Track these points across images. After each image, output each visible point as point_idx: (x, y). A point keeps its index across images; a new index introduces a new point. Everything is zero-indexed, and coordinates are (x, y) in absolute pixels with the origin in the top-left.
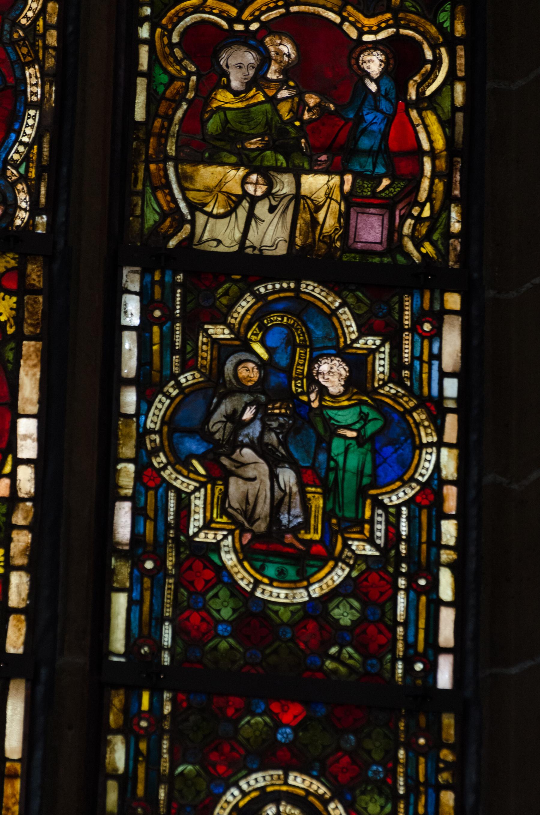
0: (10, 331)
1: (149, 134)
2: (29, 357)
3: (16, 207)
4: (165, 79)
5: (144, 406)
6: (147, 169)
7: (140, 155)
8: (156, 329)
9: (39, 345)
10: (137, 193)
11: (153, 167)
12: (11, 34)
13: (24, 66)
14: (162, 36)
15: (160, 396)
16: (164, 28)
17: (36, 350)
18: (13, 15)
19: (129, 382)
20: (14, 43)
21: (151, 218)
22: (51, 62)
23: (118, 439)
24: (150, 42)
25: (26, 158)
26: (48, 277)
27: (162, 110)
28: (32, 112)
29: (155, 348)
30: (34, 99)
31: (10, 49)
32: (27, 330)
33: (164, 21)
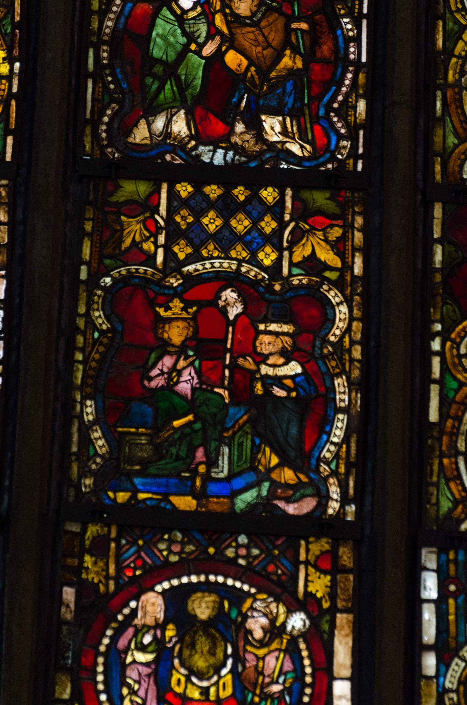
0: (326, 605)
1: (442, 433)
2: (342, 628)
3: (329, 498)
4: (454, 385)
5: (443, 668)
6: (441, 463)
7: (434, 451)
8: (451, 602)
9: (351, 617)
10: (433, 484)
11: (446, 461)
12: (321, 349)
13: (333, 377)
14: (452, 348)
15: (456, 660)
16: (453, 341)
17: (348, 621)
18: (323, 333)
19: (429, 648)
20: (324, 357)
21: (445, 505)
22: (356, 373)
23: (420, 697)
24: (442, 354)
25: (337, 456)
26: (357, 558)
27: (453, 412)
28: (341, 416)
29: (451, 618)
30: (342, 405)
31: (320, 363)
32: (340, 604)
33: (453, 336)
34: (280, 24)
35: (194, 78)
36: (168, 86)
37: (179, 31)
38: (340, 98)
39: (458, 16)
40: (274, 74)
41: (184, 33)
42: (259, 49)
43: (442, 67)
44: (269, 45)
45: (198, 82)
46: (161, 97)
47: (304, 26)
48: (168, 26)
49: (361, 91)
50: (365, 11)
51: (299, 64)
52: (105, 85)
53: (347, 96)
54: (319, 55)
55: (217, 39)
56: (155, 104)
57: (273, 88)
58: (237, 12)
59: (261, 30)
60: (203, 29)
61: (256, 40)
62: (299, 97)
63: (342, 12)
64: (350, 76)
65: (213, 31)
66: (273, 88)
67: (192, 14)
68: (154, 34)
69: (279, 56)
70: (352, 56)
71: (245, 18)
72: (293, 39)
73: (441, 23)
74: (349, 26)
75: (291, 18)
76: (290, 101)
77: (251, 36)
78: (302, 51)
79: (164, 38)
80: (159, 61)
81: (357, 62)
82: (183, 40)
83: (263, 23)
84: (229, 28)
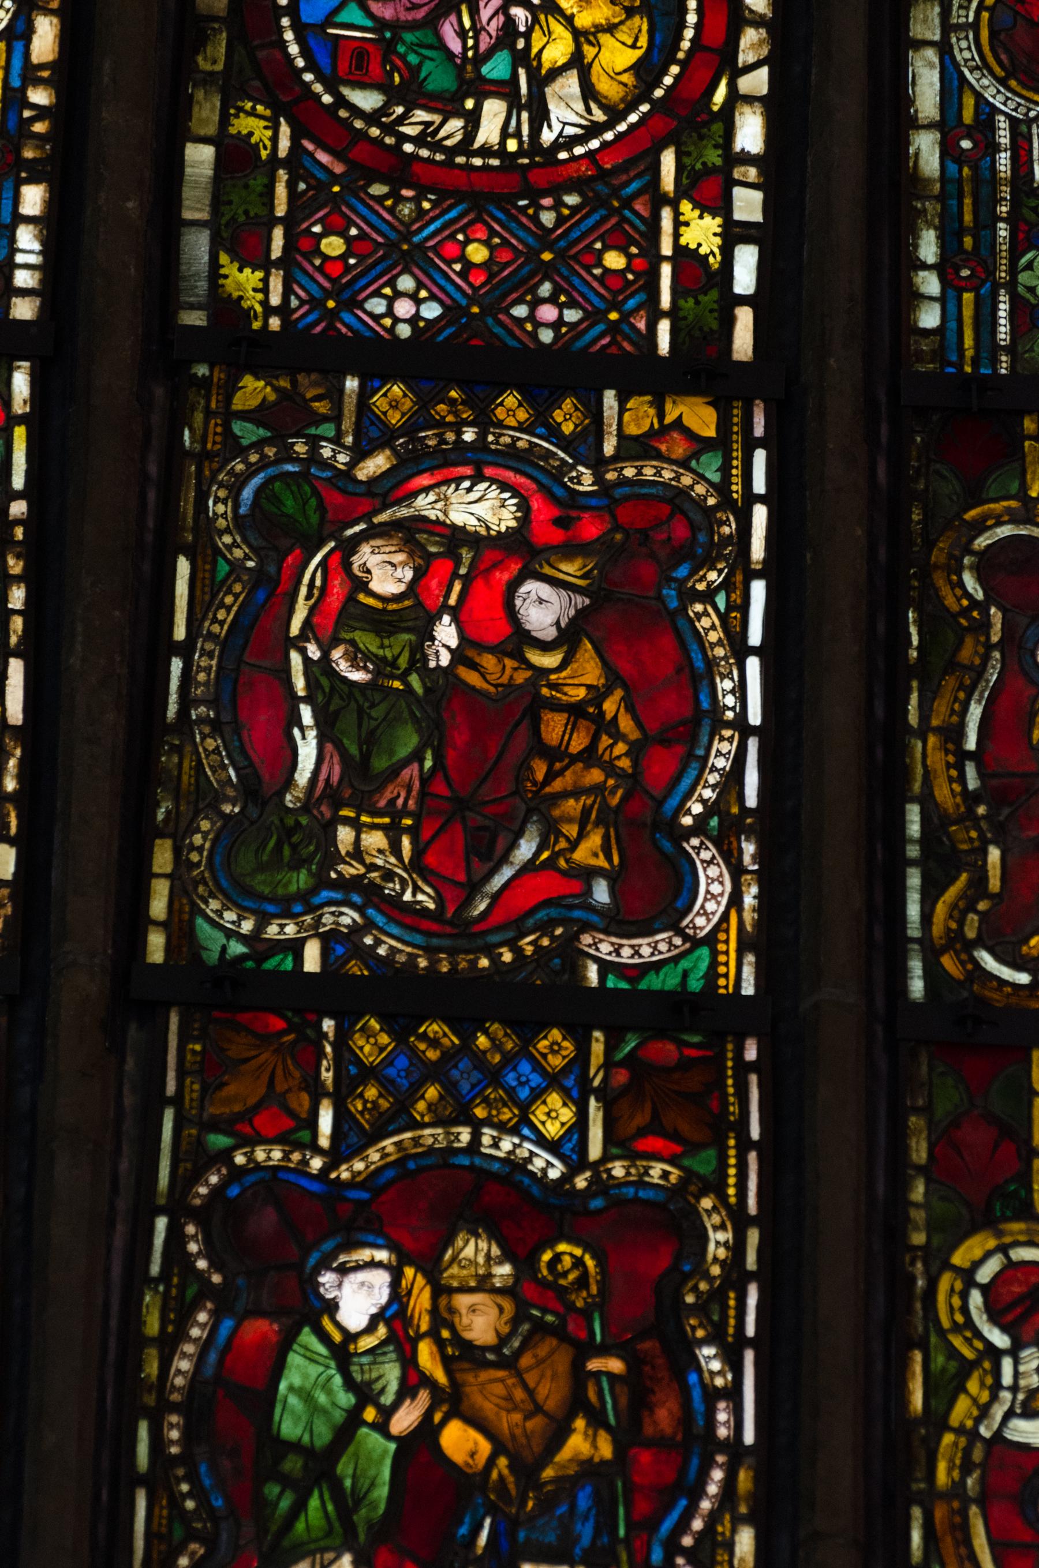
34: (562, 1361)
35: (373, 1485)
36: (314, 1502)
37: (338, 1380)
38: (697, 1525)
39: (957, 1342)
40: (548, 1473)
41: (350, 1384)
42: (517, 1417)
43: (922, 1455)
44: (538, 1409)
45: (383, 1492)
46: (300, 1526)
47: (615, 1365)
48: (314, 1370)
49: (743, 1509)
50: (750, 1330)
51: (606, 1450)
52: (176, 1501)
53: (713, 1519)
54: (649, 1430)
55: (424, 1397)
56: (286, 1543)
57: (547, 1504)
58: (468, 1335)
59: (519, 1374)
60: (391, 1374)
61: (509, 1398)
62: (606, 1523)
63: (700, 1333)
64: (718, 1475)
65: (413, 1379)
66: (547, 1504)
67: (367, 1343)
68: (283, 1386)
69: (561, 1433)
70: (722, 1432)
71: (484, 1349)
72: (592, 1395)
73: (918, 1356)
74: (716, 1365)
75: (586, 1349)
76: (586, 1532)
77: (499, 1389)
78: (612, 1420)
79: (306, 1395)
80: (295, 1447)
81: (734, 1446)
82: (346, 1399)
83: (525, 1361)
84: (449, 1372)
